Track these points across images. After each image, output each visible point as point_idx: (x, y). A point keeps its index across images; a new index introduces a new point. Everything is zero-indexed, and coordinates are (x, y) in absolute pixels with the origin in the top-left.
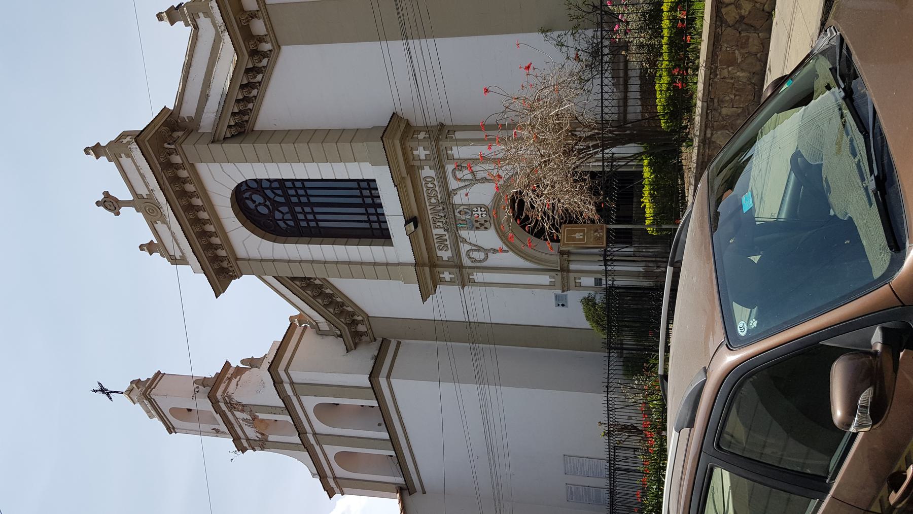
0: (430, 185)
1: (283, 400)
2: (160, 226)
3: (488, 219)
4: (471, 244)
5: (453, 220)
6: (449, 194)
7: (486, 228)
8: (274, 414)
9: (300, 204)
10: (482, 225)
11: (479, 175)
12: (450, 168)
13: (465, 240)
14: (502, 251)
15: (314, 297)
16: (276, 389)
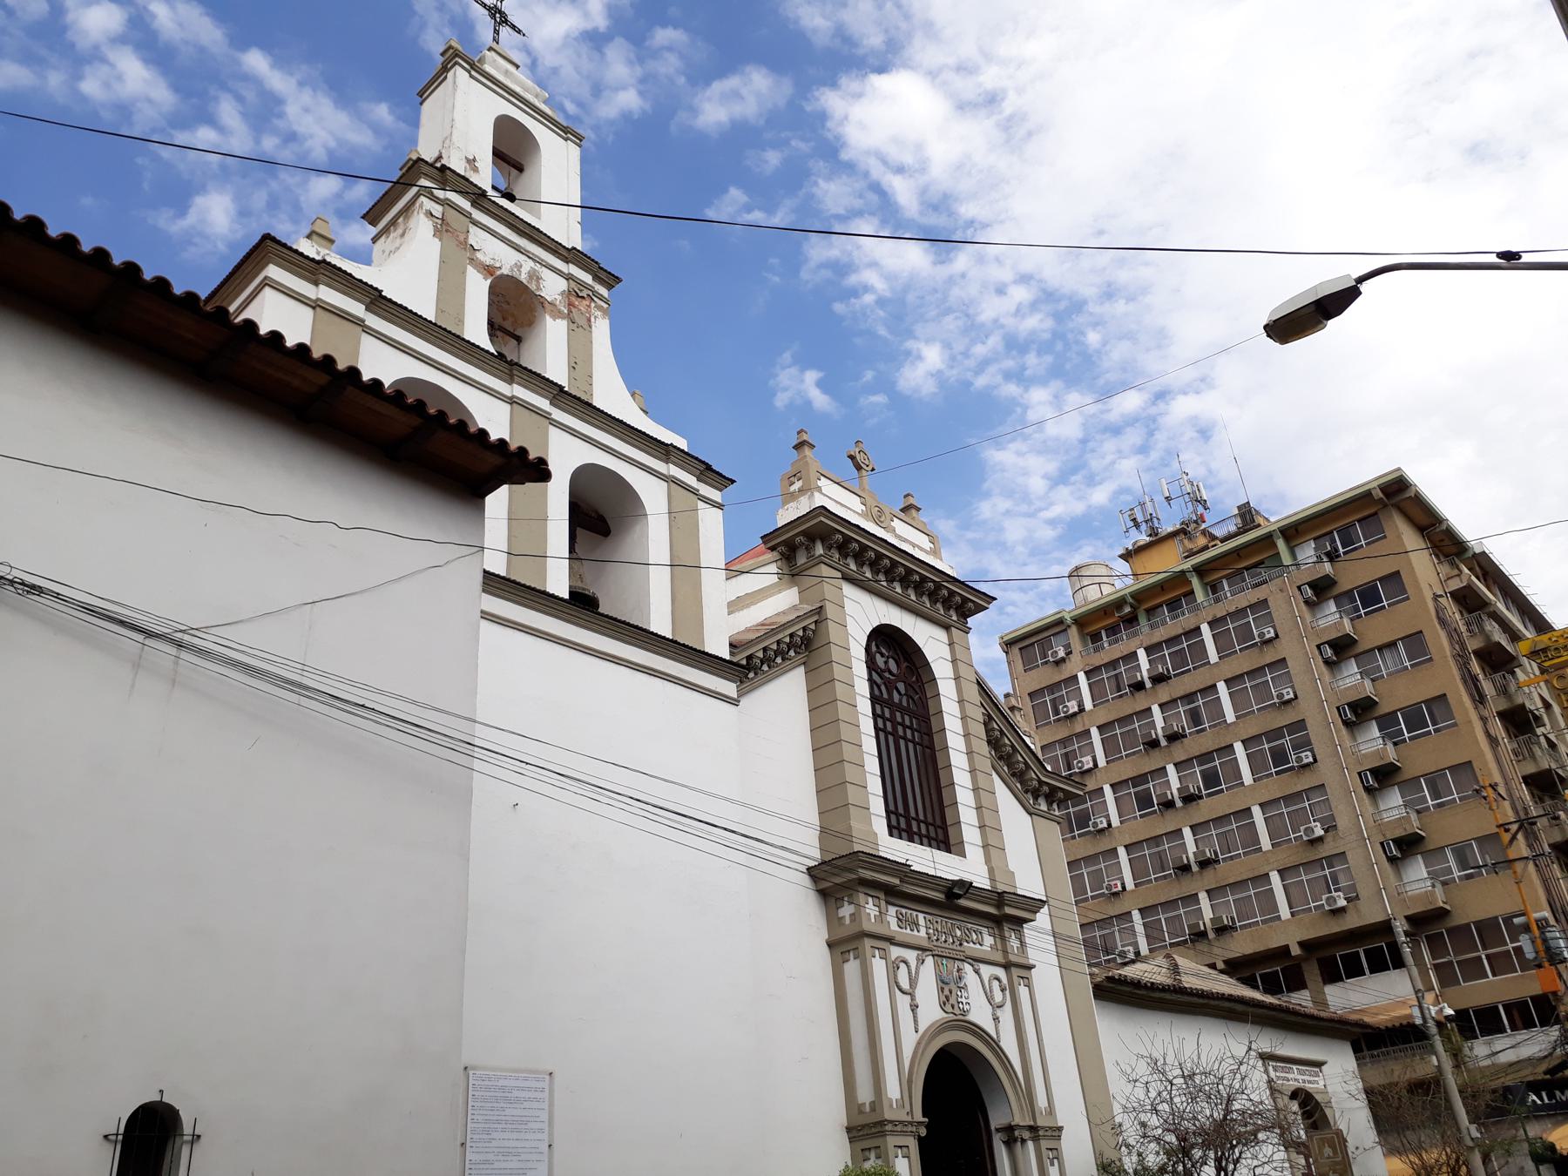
0: (975, 937)
1: (667, 445)
2: (854, 502)
3: (957, 1012)
4: (917, 969)
5: (948, 955)
6: (976, 960)
7: (943, 1005)
8: (574, 368)
9: (892, 720)
10: (947, 997)
11: (999, 1013)
12: (1001, 972)
13: (922, 963)
14: (916, 1021)
15: (778, 642)
16: (696, 459)
